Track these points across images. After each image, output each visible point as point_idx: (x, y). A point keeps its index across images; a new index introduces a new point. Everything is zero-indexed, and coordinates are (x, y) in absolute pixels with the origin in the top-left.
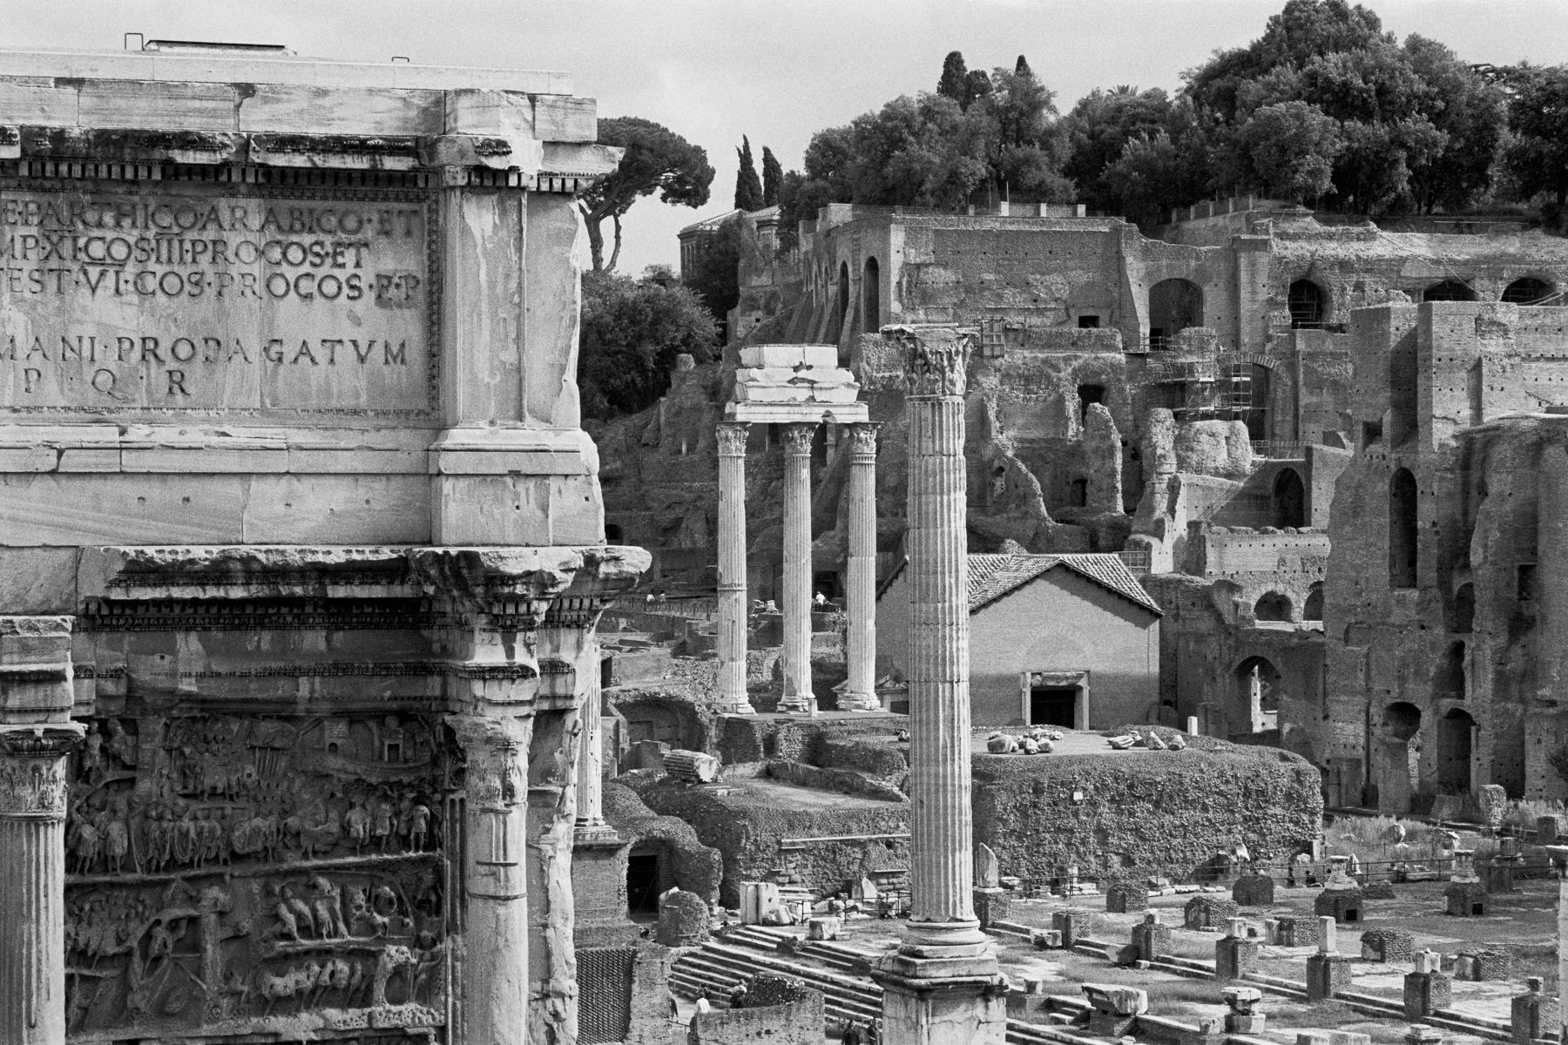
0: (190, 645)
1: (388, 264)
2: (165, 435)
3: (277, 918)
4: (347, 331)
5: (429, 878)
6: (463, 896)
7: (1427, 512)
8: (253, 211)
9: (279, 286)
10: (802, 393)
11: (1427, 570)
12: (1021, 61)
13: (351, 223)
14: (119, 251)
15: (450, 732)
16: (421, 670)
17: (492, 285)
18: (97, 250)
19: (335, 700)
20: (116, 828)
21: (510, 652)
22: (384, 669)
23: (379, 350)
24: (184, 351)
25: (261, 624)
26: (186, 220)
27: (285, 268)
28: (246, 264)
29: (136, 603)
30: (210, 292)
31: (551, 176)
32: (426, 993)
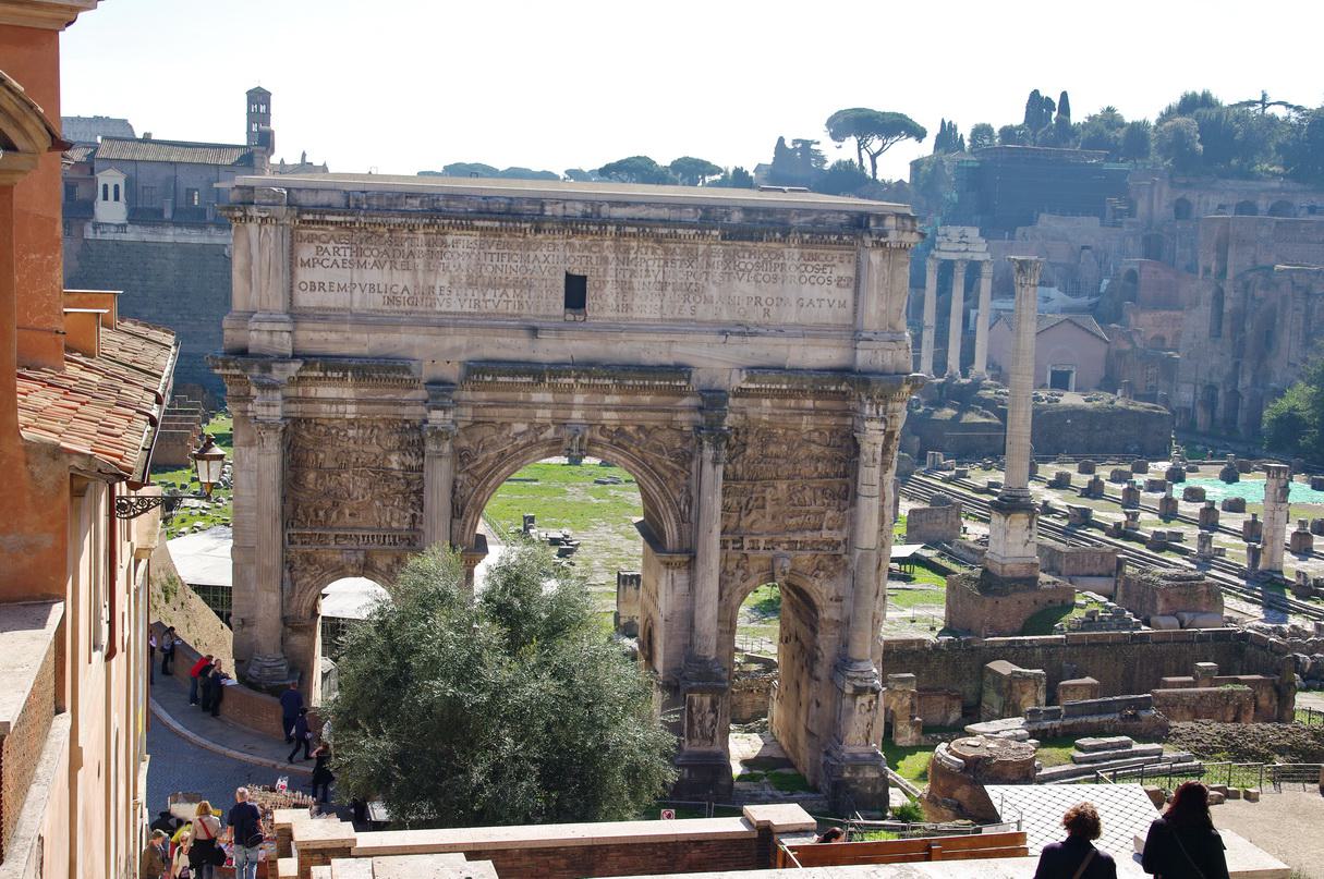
0: (767, 403)
1: (842, 274)
2: (760, 330)
3: (791, 499)
4: (825, 295)
5: (844, 488)
6: (856, 495)
7: (1228, 306)
8: (796, 252)
9: (803, 280)
10: (963, 247)
11: (1226, 328)
12: (1064, 96)
13: (829, 258)
14: (750, 267)
15: (855, 438)
16: (845, 414)
17: (878, 281)
18: (742, 266)
19: (815, 424)
20: (738, 466)
21: (878, 413)
22: (832, 412)
23: (837, 302)
24: (769, 301)
25: (791, 397)
26: (773, 256)
27: (806, 274)
28: (792, 272)
29: (749, 389)
30: (780, 281)
31: (901, 242)
32: (840, 528)
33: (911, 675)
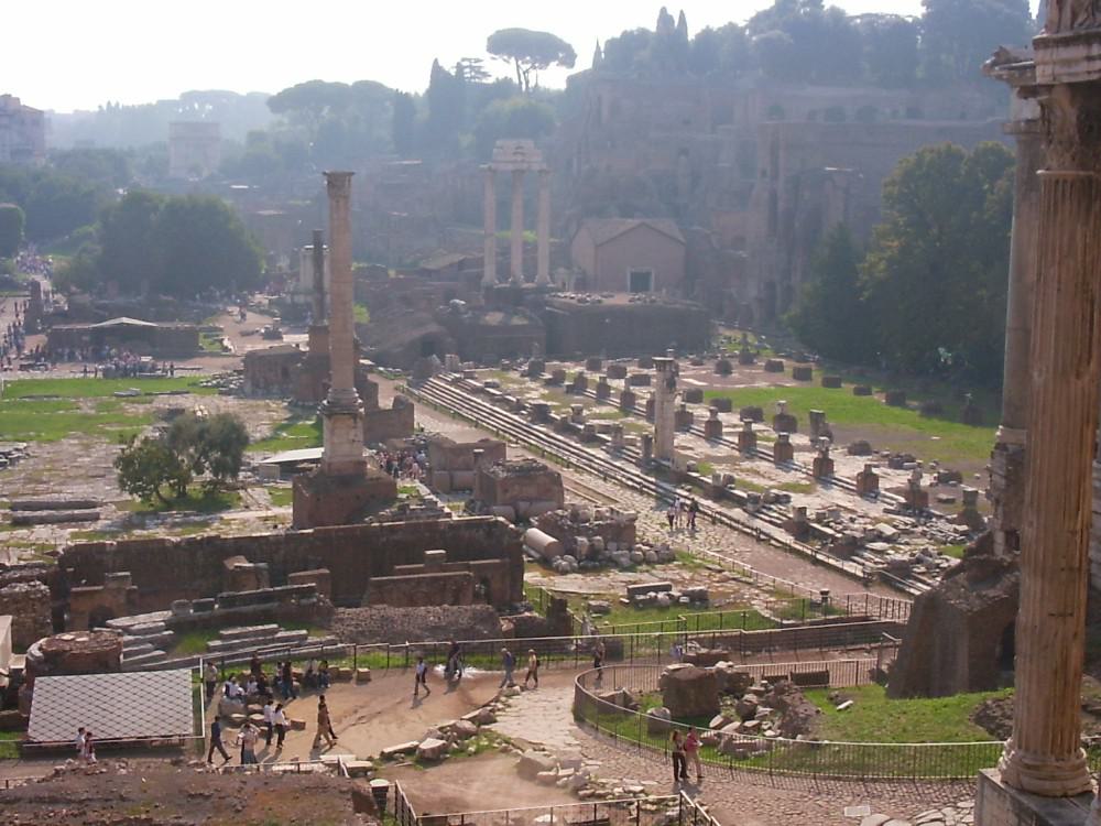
7: (781, 205)
10: (519, 158)
12: (682, 12)
33: (128, 573)
